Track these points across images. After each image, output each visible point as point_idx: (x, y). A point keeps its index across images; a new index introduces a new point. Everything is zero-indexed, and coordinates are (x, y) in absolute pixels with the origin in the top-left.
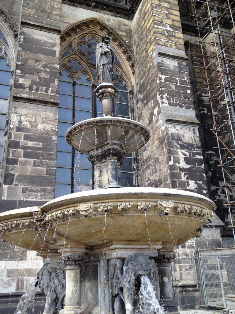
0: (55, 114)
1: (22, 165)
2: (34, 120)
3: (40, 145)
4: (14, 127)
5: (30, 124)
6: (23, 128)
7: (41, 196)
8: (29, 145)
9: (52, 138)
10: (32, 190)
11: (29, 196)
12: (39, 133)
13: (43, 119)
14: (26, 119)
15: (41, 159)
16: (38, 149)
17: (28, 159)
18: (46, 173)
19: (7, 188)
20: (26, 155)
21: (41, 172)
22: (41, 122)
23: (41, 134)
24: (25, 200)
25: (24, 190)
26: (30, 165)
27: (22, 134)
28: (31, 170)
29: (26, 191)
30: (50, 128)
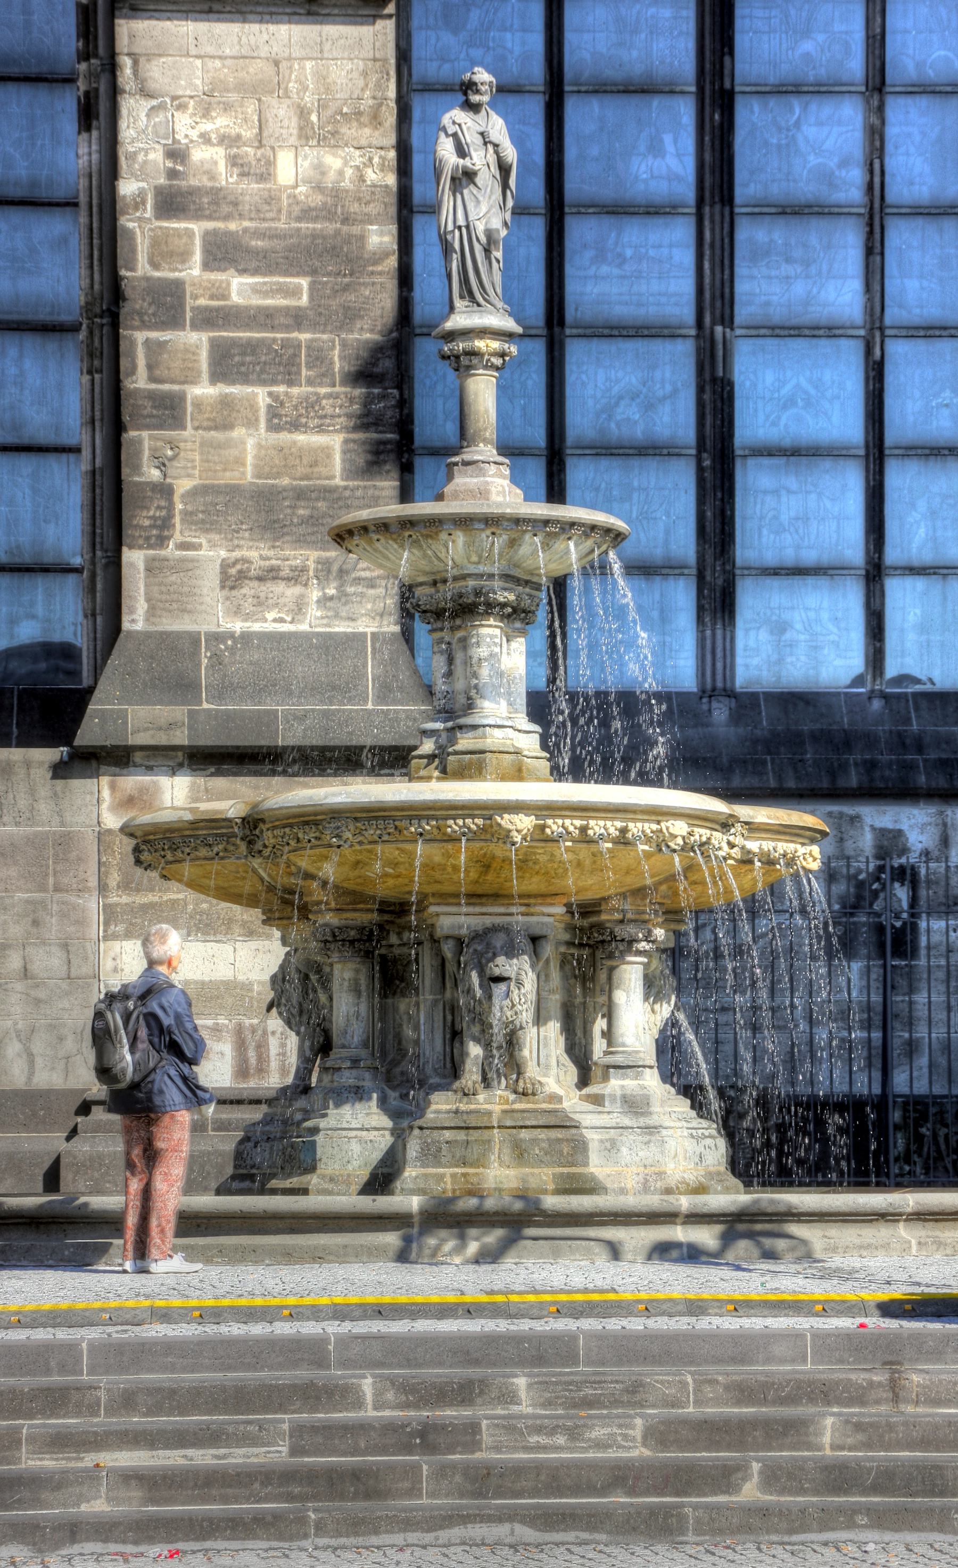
0: (378, 64)
1: (209, 429)
2: (249, 134)
3: (295, 292)
4: (142, 193)
5: (233, 161)
6: (193, 192)
7: (324, 601)
8: (236, 298)
9: (362, 238)
10: (270, 575)
11: (261, 603)
12: (290, 213)
13: (303, 113)
14: (206, 126)
15: (310, 382)
16: (289, 321)
17: (234, 390)
18: (344, 469)
19: (141, 566)
20: (226, 364)
21: (314, 464)
22: (293, 140)
23: (299, 219)
24: (238, 626)
25: (233, 571)
26: (251, 423)
27: (190, 234)
28: (256, 457)
29: (242, 576)
30: (349, 172)
